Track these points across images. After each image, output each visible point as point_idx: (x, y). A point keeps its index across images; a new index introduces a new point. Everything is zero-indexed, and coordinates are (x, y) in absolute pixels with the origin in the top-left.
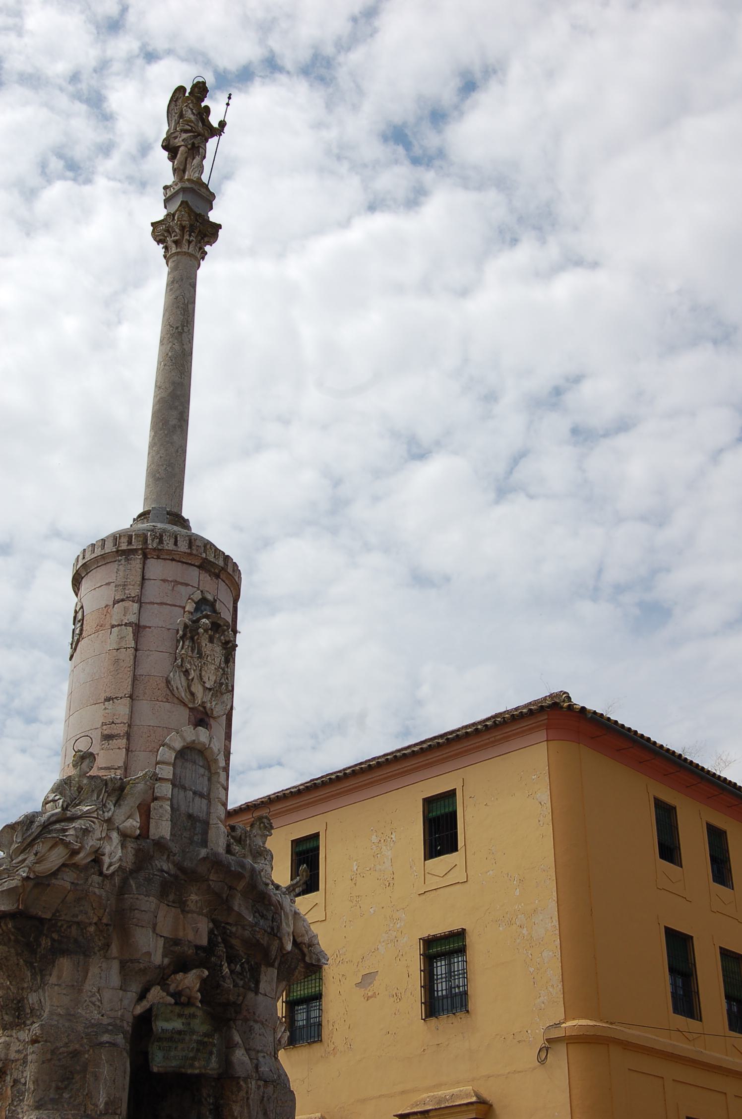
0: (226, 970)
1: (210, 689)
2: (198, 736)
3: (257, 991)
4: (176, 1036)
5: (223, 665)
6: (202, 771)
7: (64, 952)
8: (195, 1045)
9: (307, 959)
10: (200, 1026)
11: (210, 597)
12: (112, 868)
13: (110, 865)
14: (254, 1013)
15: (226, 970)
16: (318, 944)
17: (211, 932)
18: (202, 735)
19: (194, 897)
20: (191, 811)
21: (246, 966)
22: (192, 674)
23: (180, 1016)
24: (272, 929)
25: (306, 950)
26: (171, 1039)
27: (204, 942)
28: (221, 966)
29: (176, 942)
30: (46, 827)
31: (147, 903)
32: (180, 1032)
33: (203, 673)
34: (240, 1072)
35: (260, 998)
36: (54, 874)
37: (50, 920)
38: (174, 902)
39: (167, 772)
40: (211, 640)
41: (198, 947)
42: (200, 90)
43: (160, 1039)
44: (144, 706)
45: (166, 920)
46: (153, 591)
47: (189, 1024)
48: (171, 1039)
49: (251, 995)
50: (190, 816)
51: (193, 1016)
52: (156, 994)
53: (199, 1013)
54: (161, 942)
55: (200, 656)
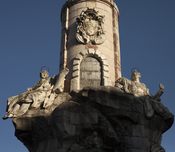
1: (92, 35)
2: (88, 51)
3: (131, 135)
5: (97, 26)
6: (95, 63)
9: (165, 119)
12: (47, 106)
13: (46, 104)
14: (131, 145)
15: (111, 130)
16: (168, 111)
17: (99, 118)
20: (90, 78)
22: (84, 32)
25: (162, 115)
27: (97, 121)
28: (107, 129)
33: (88, 31)
37: (32, 131)
38: (77, 110)
50: (90, 80)
54: (74, 127)
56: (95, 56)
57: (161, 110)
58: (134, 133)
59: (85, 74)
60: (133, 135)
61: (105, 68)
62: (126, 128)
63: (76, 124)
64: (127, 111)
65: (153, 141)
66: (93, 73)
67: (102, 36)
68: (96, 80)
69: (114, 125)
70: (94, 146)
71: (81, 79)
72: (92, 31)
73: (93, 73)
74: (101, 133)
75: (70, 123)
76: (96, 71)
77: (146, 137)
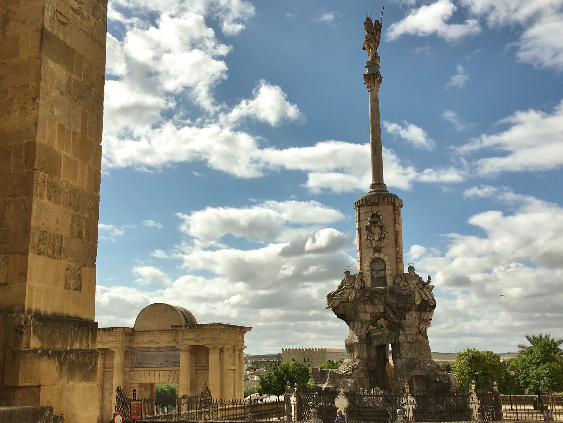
0: (392, 316)
3: (405, 319)
7: (351, 321)
10: (387, 332)
11: (375, 213)
15: (392, 316)
17: (384, 308)
18: (377, 255)
27: (383, 311)
29: (374, 313)
30: (334, 295)
31: (360, 307)
34: (401, 342)
35: (406, 321)
36: (339, 305)
39: (369, 268)
40: (375, 227)
41: (381, 313)
42: (368, 20)
44: (363, 251)
45: (370, 309)
46: (363, 217)
49: (402, 321)
50: (377, 278)
52: (371, 327)
54: (369, 314)
55: (372, 233)
56: (380, 258)
57: (427, 299)
59: (374, 273)
61: (388, 267)
62: (402, 314)
66: (380, 272)
67: (384, 240)
68: (381, 277)
69: (394, 313)
70: (382, 327)
71: (372, 277)
72: (376, 237)
73: (380, 272)
74: (386, 318)
75: (366, 312)
76: (382, 270)
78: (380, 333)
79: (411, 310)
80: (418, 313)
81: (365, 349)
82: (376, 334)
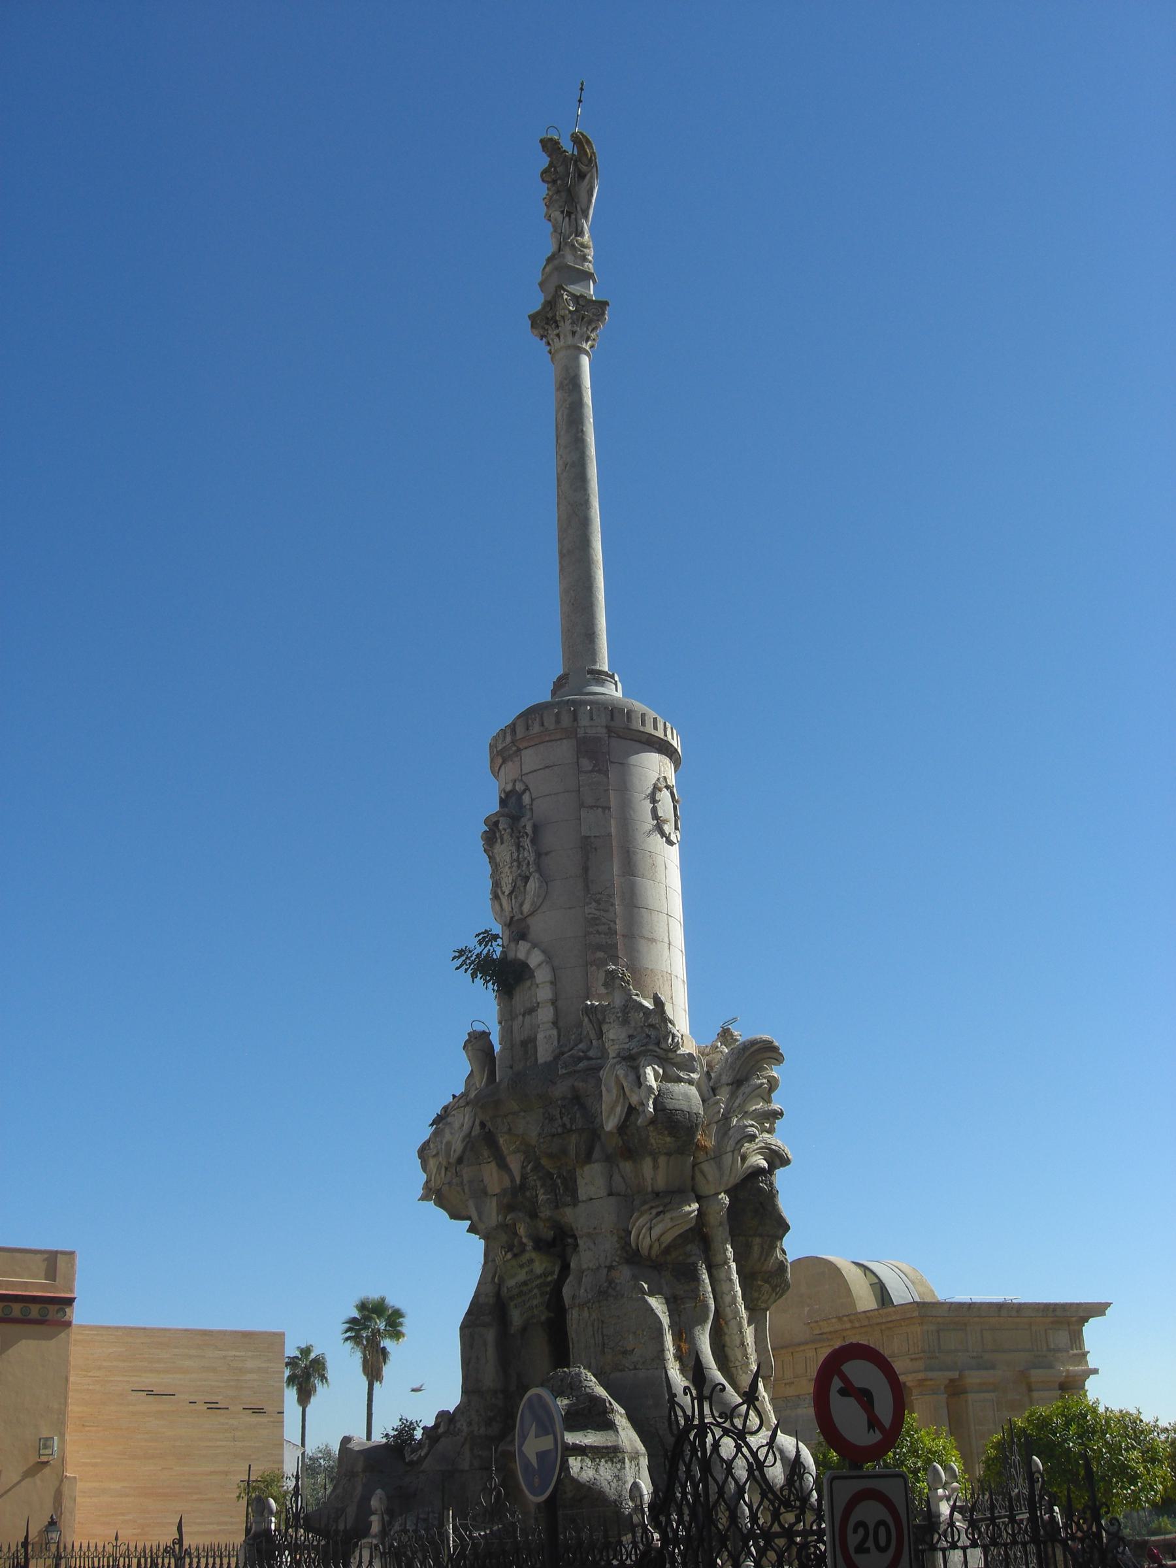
3: (575, 1202)
4: (525, 1289)
8: (535, 1291)
19: (501, 1141)
21: (559, 1181)
23: (521, 1266)
24: (564, 1125)
26: (521, 1294)
28: (537, 1195)
32: (525, 1283)
43: (512, 1298)
47: (532, 1271)
48: (521, 1294)
49: (568, 1211)
51: (531, 1261)
53: (533, 1255)
58: (582, 1193)
60: (580, 1199)
63: (497, 1191)
64: (554, 1136)
65: (650, 1189)
66: (528, 1017)
75: (485, 1193)
77: (610, 1194)
78: (522, 1276)
79: (588, 1159)
80: (627, 1166)
81: (491, 1351)
82: (511, 1283)
